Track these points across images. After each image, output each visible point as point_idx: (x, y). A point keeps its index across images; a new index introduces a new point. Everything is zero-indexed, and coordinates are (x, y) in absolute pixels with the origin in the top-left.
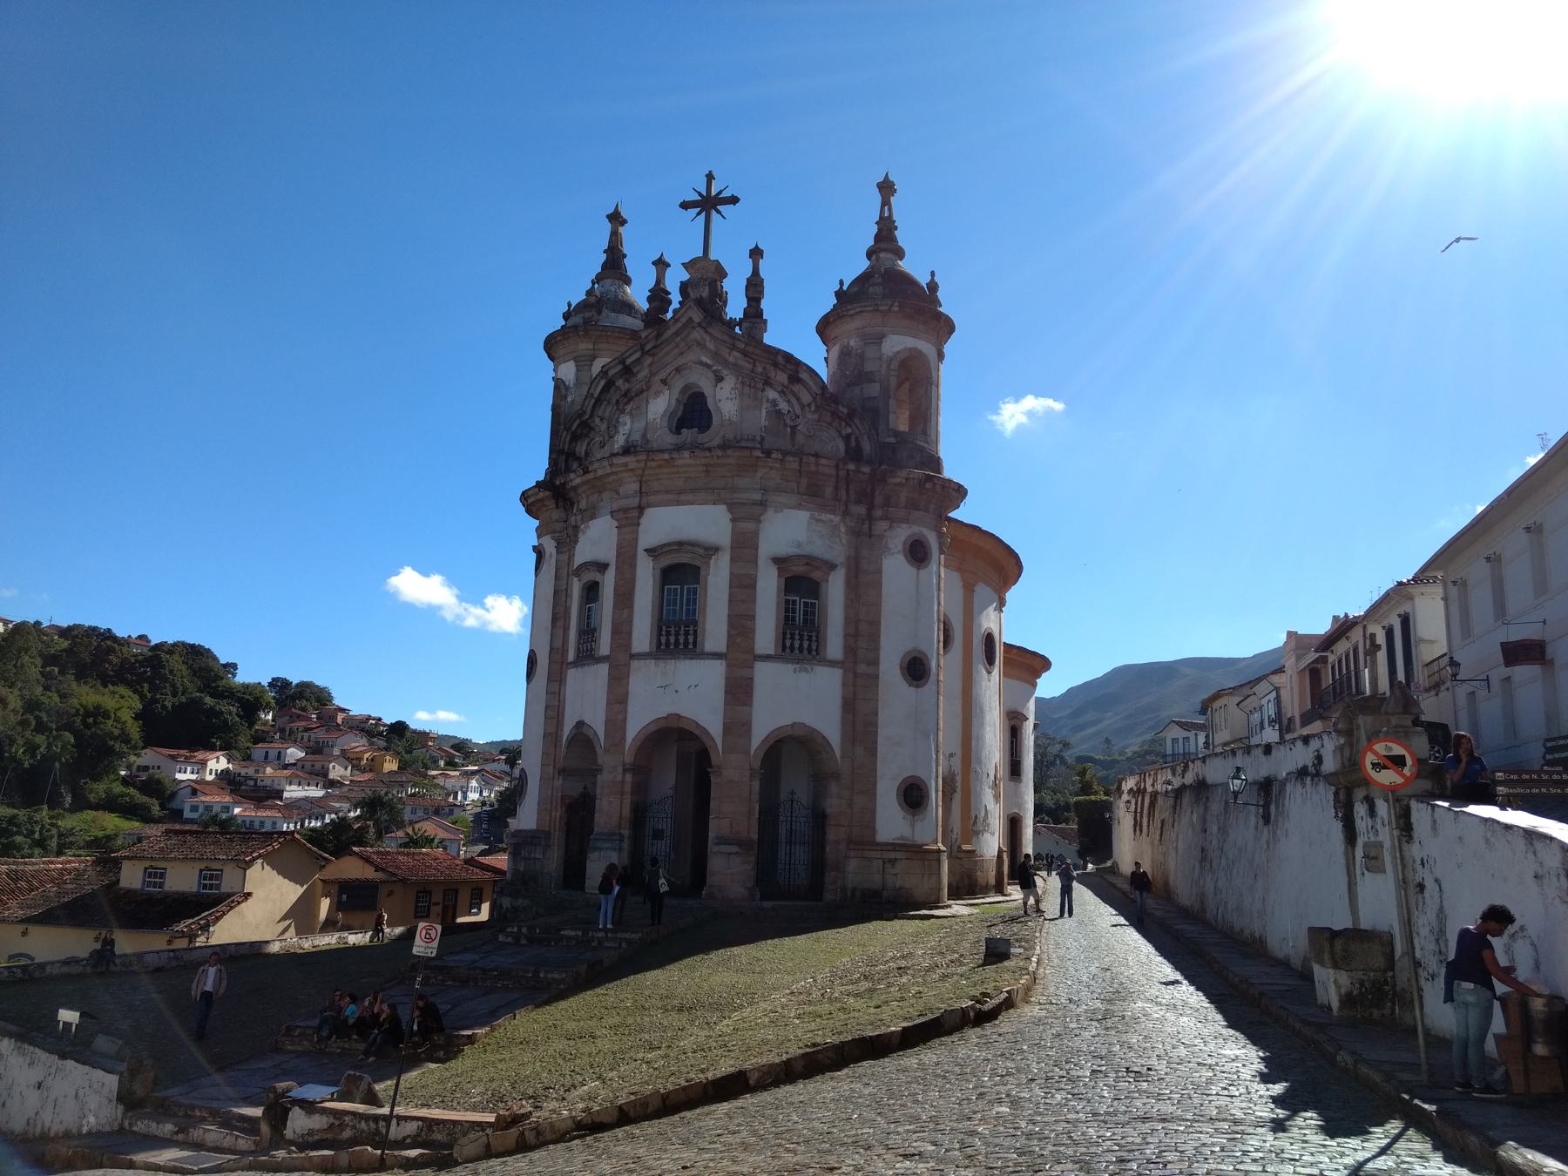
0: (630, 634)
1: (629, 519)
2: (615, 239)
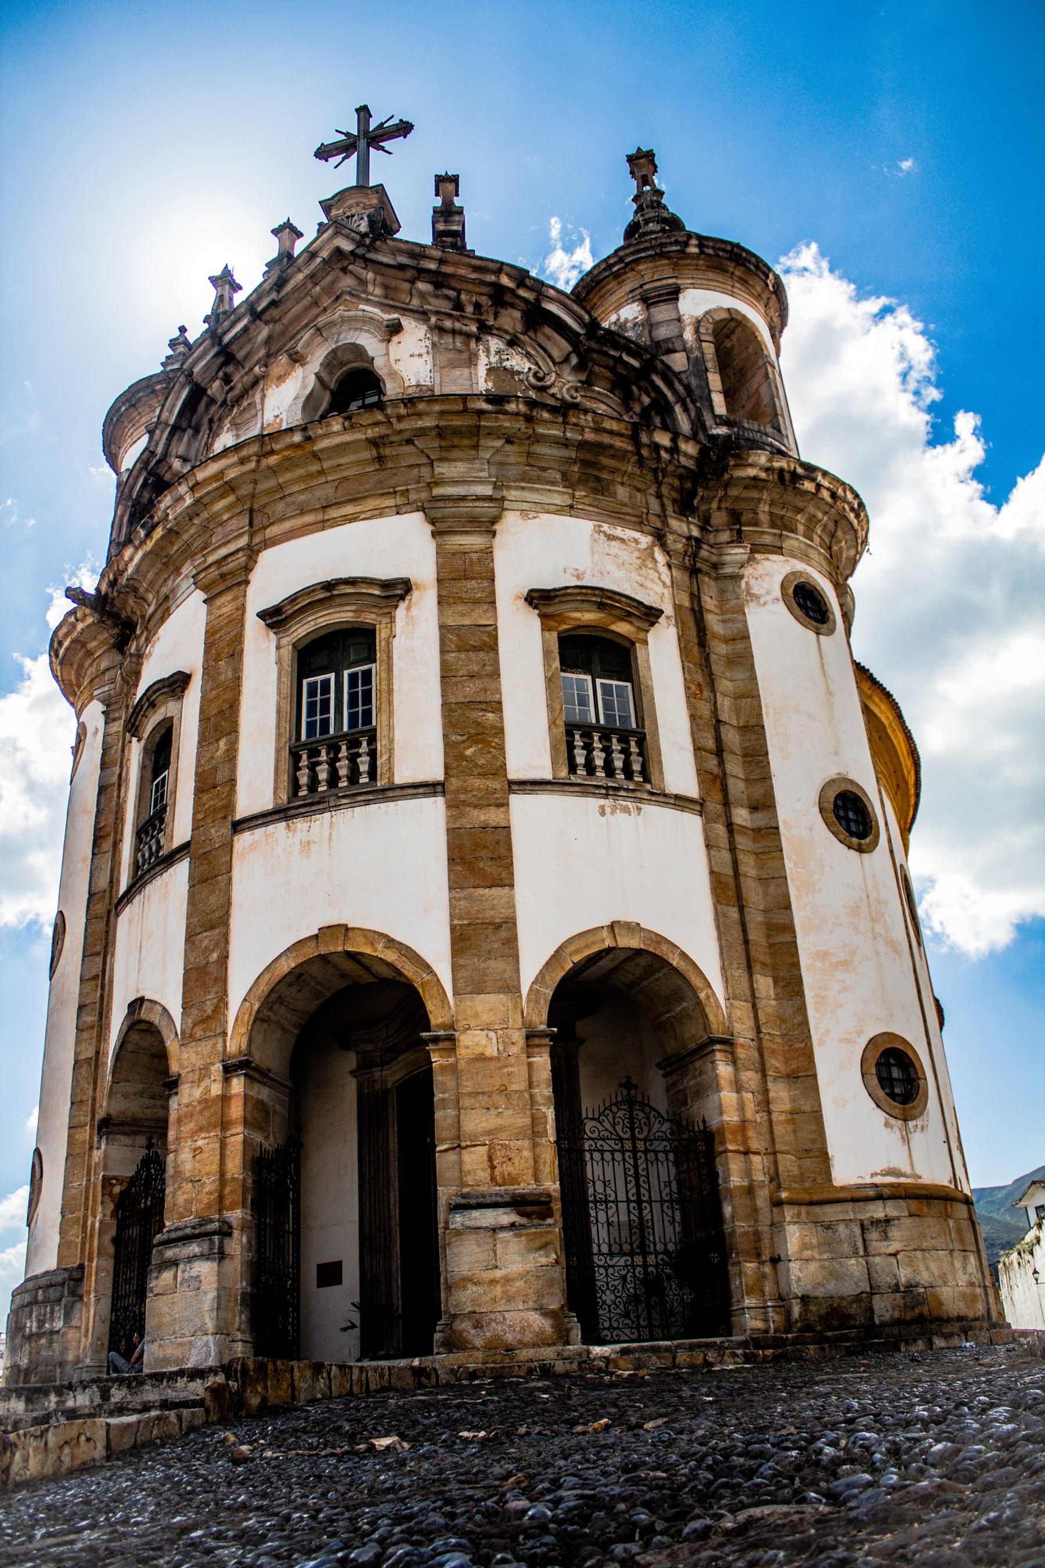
0: (232, 782)
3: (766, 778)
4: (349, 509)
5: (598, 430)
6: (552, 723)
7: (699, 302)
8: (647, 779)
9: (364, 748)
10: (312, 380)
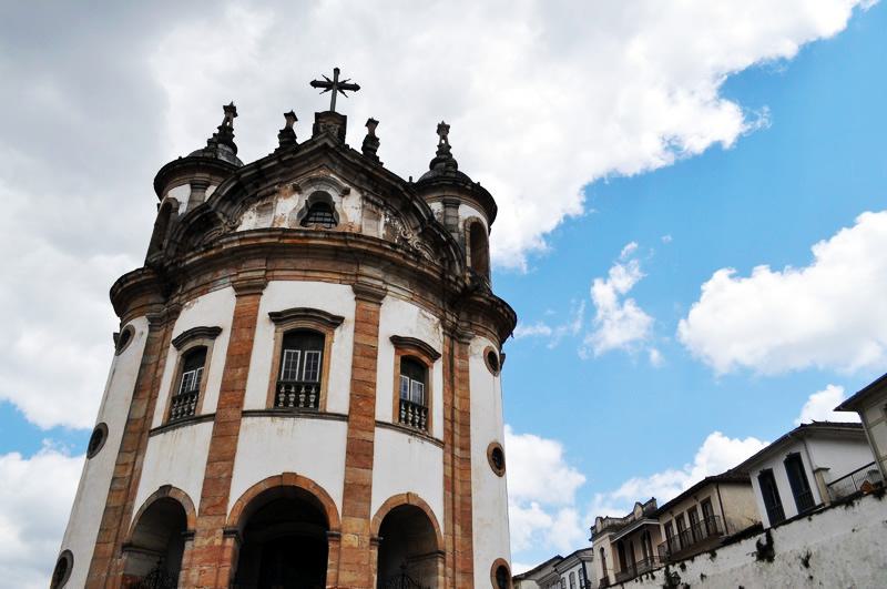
1: (250, 290)
2: (228, 119)
3: (468, 436)
4: (318, 275)
5: (429, 269)
6: (395, 398)
7: (467, 212)
8: (427, 430)
9: (313, 391)
10: (303, 204)
